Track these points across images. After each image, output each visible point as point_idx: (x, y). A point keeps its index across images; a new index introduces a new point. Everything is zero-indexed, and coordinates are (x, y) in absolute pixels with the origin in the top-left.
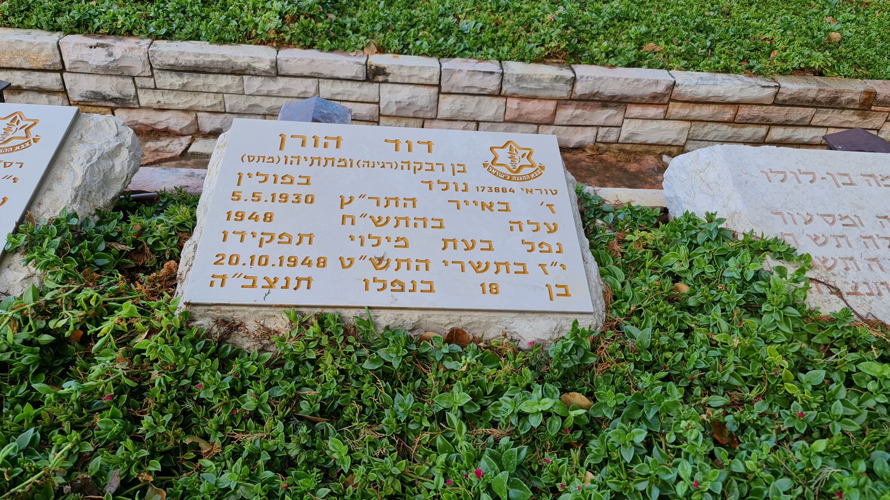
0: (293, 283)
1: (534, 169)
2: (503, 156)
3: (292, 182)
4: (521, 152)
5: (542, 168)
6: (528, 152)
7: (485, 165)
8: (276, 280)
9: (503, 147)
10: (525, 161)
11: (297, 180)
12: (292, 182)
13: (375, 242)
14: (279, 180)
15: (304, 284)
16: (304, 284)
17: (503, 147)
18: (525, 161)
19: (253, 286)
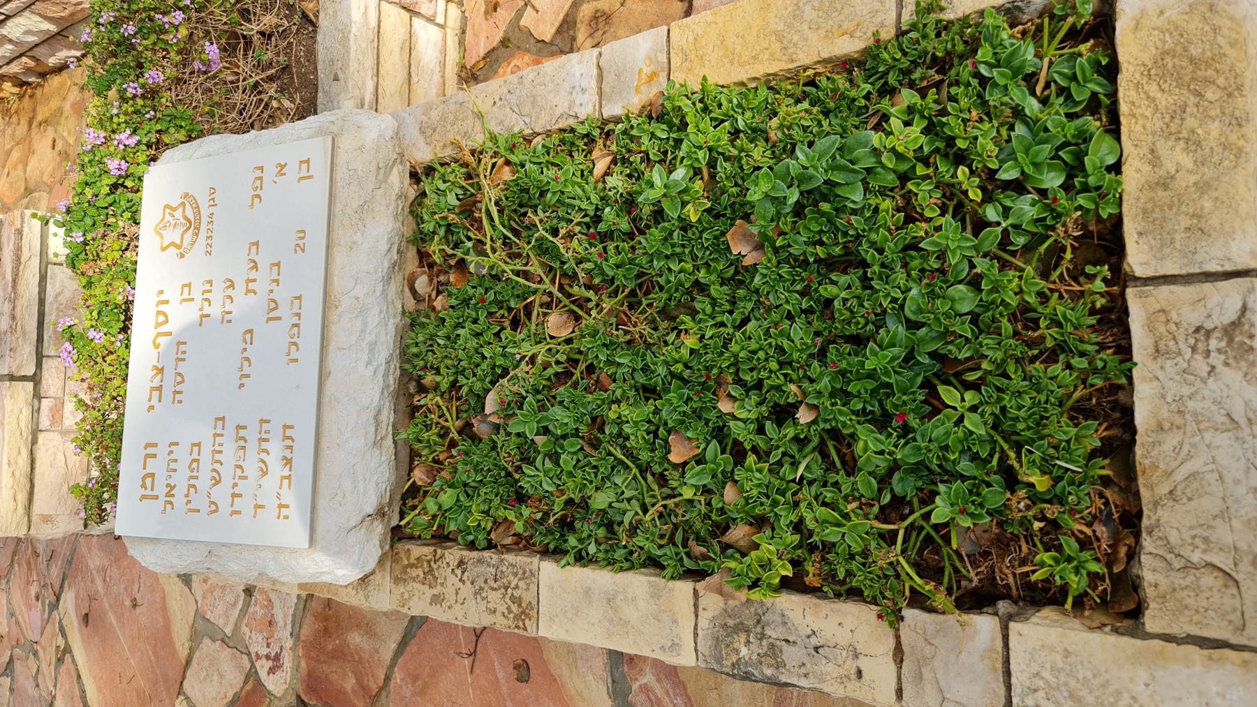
0: (289, 442)
1: (188, 205)
2: (173, 235)
3: (197, 461)
4: (168, 218)
5: (186, 195)
6: (168, 211)
7: (182, 256)
8: (285, 458)
9: (162, 236)
10: (178, 214)
11: (195, 456)
12: (197, 461)
13: (246, 363)
14: (195, 474)
15: (289, 432)
16: (289, 432)
17: (162, 236)
18: (178, 214)
19: (289, 477)
